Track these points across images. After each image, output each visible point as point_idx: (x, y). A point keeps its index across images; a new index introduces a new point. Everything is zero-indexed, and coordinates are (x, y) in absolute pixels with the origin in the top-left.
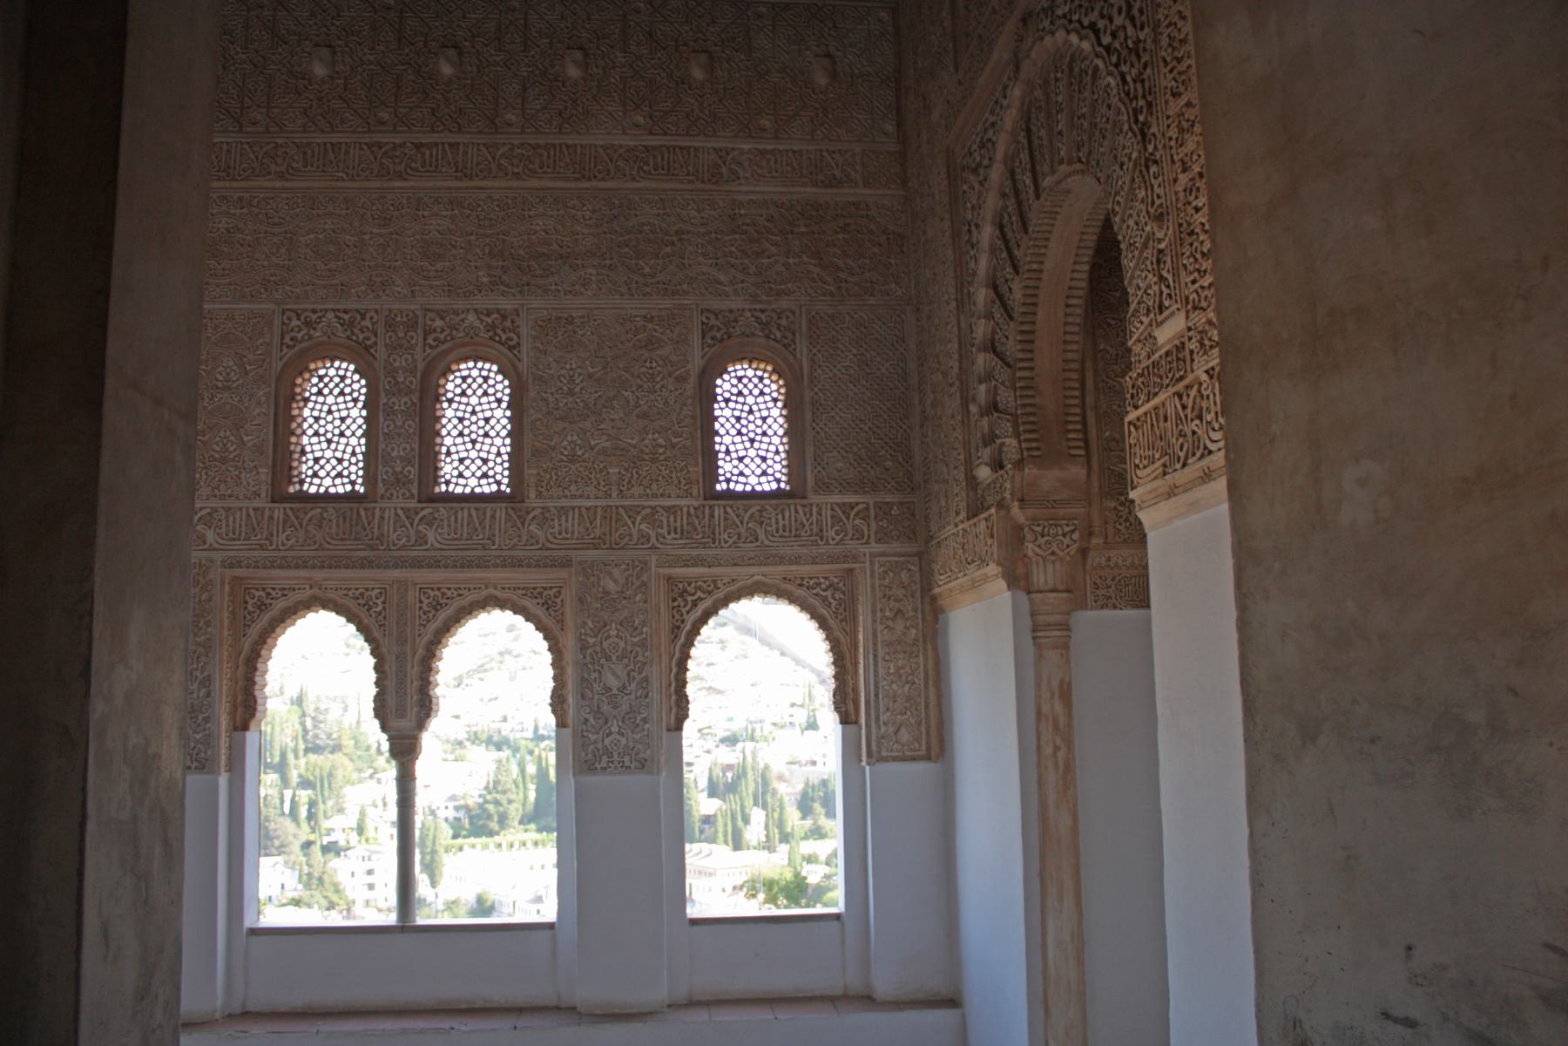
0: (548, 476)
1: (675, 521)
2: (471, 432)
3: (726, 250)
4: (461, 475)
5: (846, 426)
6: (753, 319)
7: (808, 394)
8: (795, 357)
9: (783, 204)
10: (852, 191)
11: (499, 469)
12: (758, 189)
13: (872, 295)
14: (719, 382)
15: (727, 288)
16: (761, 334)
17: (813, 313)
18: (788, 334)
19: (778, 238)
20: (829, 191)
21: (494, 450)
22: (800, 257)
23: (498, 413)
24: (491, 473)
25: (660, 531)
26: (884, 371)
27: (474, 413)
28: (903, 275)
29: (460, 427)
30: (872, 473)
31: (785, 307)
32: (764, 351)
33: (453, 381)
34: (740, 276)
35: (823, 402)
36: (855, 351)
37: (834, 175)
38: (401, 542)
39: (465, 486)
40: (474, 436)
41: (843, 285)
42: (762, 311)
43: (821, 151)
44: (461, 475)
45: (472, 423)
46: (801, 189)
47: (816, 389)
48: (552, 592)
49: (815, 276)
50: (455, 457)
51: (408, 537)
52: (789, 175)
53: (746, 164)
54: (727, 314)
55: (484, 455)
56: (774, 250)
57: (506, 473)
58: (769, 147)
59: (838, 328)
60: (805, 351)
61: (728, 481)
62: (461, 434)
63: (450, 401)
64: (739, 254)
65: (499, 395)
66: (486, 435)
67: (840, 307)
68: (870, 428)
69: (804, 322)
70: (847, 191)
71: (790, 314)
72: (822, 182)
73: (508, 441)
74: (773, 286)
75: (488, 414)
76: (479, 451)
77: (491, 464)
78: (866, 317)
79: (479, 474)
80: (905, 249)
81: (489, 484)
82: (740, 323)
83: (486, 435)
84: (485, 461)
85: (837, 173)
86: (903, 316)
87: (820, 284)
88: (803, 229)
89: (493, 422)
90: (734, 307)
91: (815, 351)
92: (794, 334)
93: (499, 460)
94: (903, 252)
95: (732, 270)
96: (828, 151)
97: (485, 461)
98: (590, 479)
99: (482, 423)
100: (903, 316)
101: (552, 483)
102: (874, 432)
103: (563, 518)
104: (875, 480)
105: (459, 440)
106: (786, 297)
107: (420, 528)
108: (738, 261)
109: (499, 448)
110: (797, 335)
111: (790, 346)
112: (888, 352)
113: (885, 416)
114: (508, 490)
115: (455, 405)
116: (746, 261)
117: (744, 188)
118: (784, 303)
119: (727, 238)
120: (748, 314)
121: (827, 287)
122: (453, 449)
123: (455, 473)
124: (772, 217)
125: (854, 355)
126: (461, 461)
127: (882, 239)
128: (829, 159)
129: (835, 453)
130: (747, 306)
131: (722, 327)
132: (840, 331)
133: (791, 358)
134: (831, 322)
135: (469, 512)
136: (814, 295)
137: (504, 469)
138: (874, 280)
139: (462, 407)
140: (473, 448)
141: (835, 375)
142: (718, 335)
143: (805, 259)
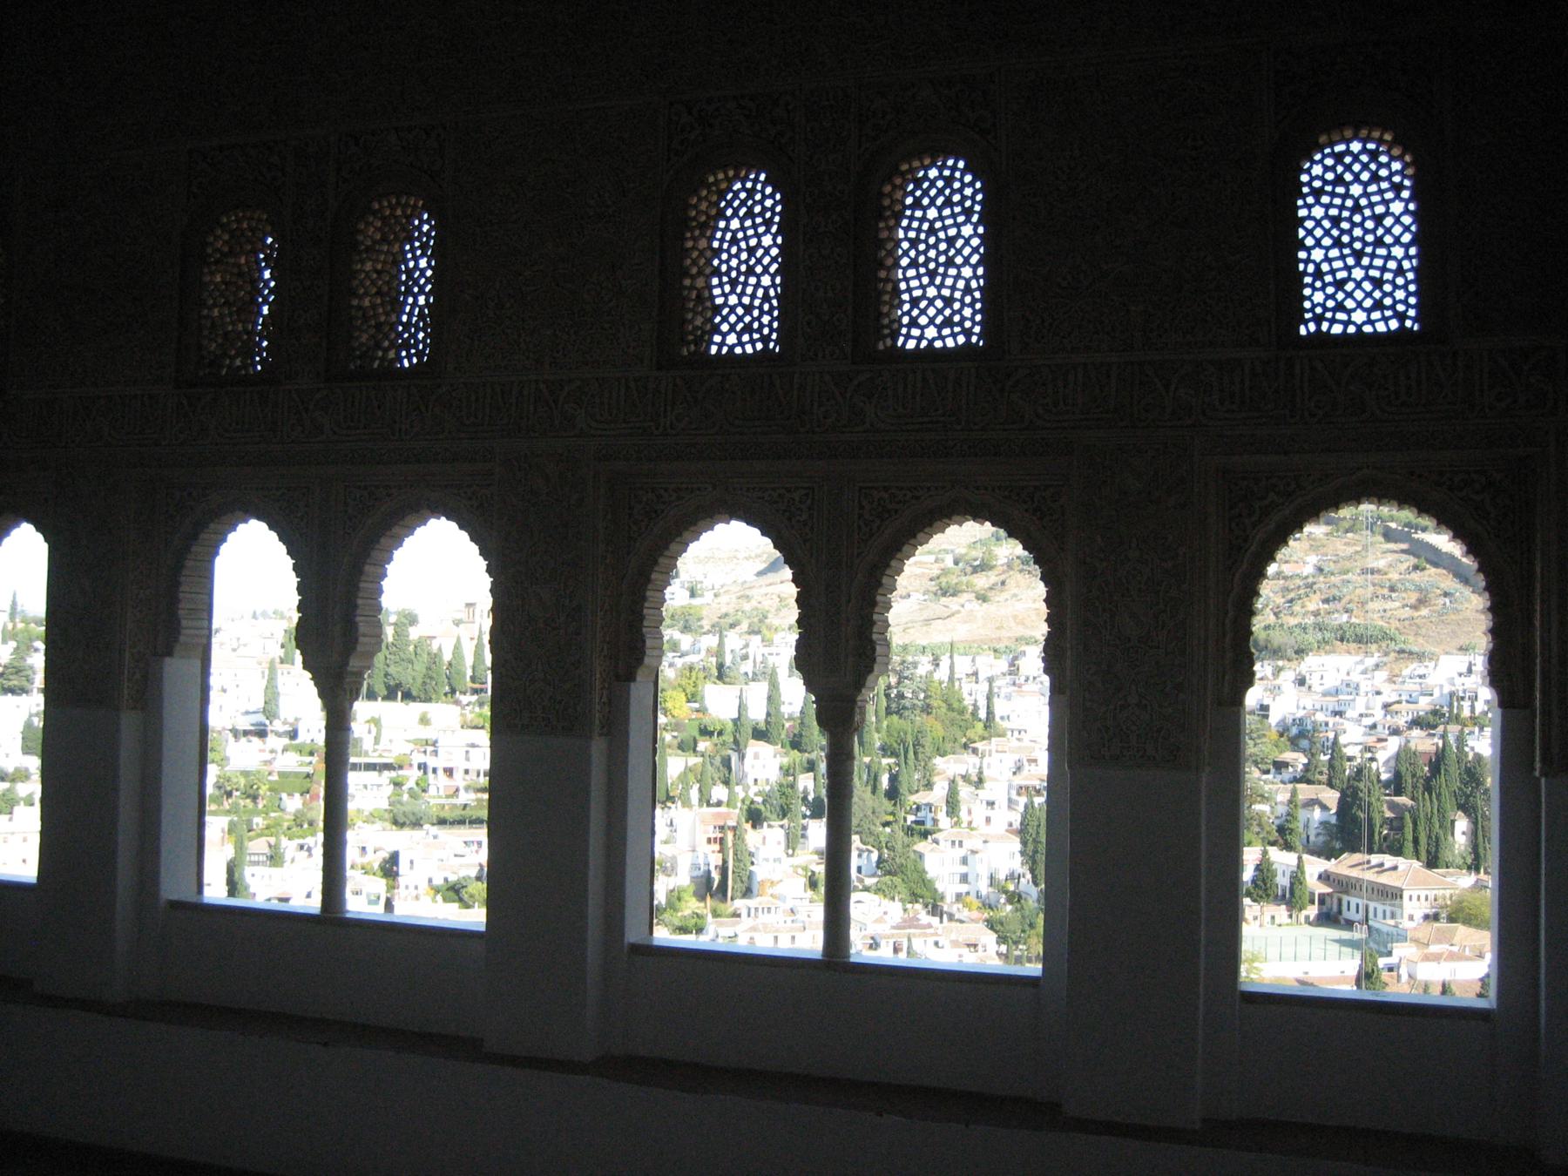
2: (1353, 240)
4: (1340, 307)
21: (1392, 265)
23: (1397, 207)
24: (1388, 301)
27: (1357, 208)
33: (1321, 161)
39: (1346, 324)
40: (1358, 245)
44: (1340, 307)
45: (1354, 225)
50: (1328, 279)
55: (1374, 273)
57: (1412, 300)
62: (1337, 243)
63: (1317, 193)
66: (1379, 242)
73: (1413, 251)
75: (1380, 209)
77: (1388, 288)
79: (1368, 303)
81: (1385, 319)
83: (1379, 242)
84: (1379, 284)
89: (1388, 221)
93: (1400, 281)
99: (1370, 225)
105: (1334, 253)
115: (1325, 199)
126: (1339, 285)
137: (1409, 294)
139: (1337, 201)
140: (1358, 264)
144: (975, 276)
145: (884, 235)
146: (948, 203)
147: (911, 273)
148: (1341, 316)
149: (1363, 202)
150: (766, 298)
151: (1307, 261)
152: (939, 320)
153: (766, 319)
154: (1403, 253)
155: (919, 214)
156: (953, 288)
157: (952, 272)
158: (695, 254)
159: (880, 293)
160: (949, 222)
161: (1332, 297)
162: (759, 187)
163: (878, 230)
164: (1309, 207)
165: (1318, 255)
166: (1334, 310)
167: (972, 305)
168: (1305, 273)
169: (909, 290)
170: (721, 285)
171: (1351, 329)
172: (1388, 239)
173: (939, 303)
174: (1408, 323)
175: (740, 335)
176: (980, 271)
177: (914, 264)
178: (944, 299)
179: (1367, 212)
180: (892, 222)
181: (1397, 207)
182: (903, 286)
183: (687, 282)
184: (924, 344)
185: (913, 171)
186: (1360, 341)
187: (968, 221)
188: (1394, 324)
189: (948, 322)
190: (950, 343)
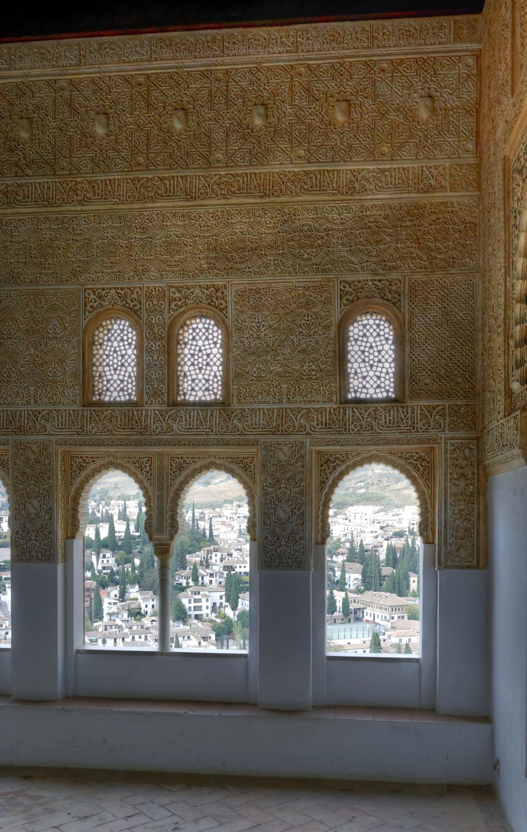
0: (294, 389)
4: (364, 387)
10: (442, 194)
13: (453, 267)
14: (351, 328)
15: (357, 266)
17: (413, 281)
18: (396, 295)
19: (392, 231)
21: (384, 370)
22: (405, 243)
25: (380, 422)
26: (459, 318)
27: (371, 347)
29: (363, 357)
31: (394, 277)
34: (365, 258)
35: (418, 340)
36: (440, 306)
39: (367, 394)
40: (371, 362)
41: (434, 260)
42: (380, 281)
44: (364, 387)
45: (370, 354)
49: (415, 255)
51: (294, 426)
54: (357, 284)
55: (378, 374)
56: (388, 239)
59: (429, 290)
60: (407, 307)
62: (364, 361)
63: (356, 340)
65: (387, 336)
67: (431, 276)
70: (438, 194)
71: (397, 282)
76: (375, 372)
78: (448, 282)
79: (375, 386)
80: (477, 234)
81: (382, 392)
82: (365, 289)
84: (379, 378)
86: (474, 280)
87: (418, 261)
88: (408, 224)
90: (361, 278)
91: (413, 306)
92: (400, 295)
93: (387, 377)
97: (379, 378)
98: (319, 390)
99: (376, 354)
103: (387, 415)
105: (362, 365)
106: (395, 271)
107: (368, 420)
109: (387, 369)
110: (402, 296)
112: (462, 305)
114: (393, 396)
115: (359, 343)
116: (370, 247)
118: (394, 275)
120: (370, 283)
123: (360, 386)
127: (461, 227)
130: (370, 278)
131: (353, 292)
132: (431, 292)
133: (397, 311)
135: (398, 409)
138: (455, 256)
139: (364, 344)
141: (426, 322)
143: (409, 244)
145: (180, 351)
146: (207, 339)
147: (192, 368)
148: (364, 390)
149: (374, 345)
150: (130, 377)
151: (351, 368)
152: (203, 388)
153: (130, 386)
155: (194, 343)
157: (209, 368)
158: (98, 357)
159: (178, 377)
160: (207, 347)
161: (361, 383)
162: (126, 328)
164: (353, 346)
165: (356, 365)
166: (362, 388)
167: (217, 382)
168: (351, 373)
169: (191, 375)
170: (110, 370)
171: (368, 396)
172: (383, 360)
173: (204, 381)
174: (390, 394)
175: (119, 392)
177: (193, 364)
179: (375, 349)
180: (183, 346)
182: (188, 374)
183: (95, 369)
185: (191, 324)
186: (371, 401)
187: (215, 347)
188: (385, 394)
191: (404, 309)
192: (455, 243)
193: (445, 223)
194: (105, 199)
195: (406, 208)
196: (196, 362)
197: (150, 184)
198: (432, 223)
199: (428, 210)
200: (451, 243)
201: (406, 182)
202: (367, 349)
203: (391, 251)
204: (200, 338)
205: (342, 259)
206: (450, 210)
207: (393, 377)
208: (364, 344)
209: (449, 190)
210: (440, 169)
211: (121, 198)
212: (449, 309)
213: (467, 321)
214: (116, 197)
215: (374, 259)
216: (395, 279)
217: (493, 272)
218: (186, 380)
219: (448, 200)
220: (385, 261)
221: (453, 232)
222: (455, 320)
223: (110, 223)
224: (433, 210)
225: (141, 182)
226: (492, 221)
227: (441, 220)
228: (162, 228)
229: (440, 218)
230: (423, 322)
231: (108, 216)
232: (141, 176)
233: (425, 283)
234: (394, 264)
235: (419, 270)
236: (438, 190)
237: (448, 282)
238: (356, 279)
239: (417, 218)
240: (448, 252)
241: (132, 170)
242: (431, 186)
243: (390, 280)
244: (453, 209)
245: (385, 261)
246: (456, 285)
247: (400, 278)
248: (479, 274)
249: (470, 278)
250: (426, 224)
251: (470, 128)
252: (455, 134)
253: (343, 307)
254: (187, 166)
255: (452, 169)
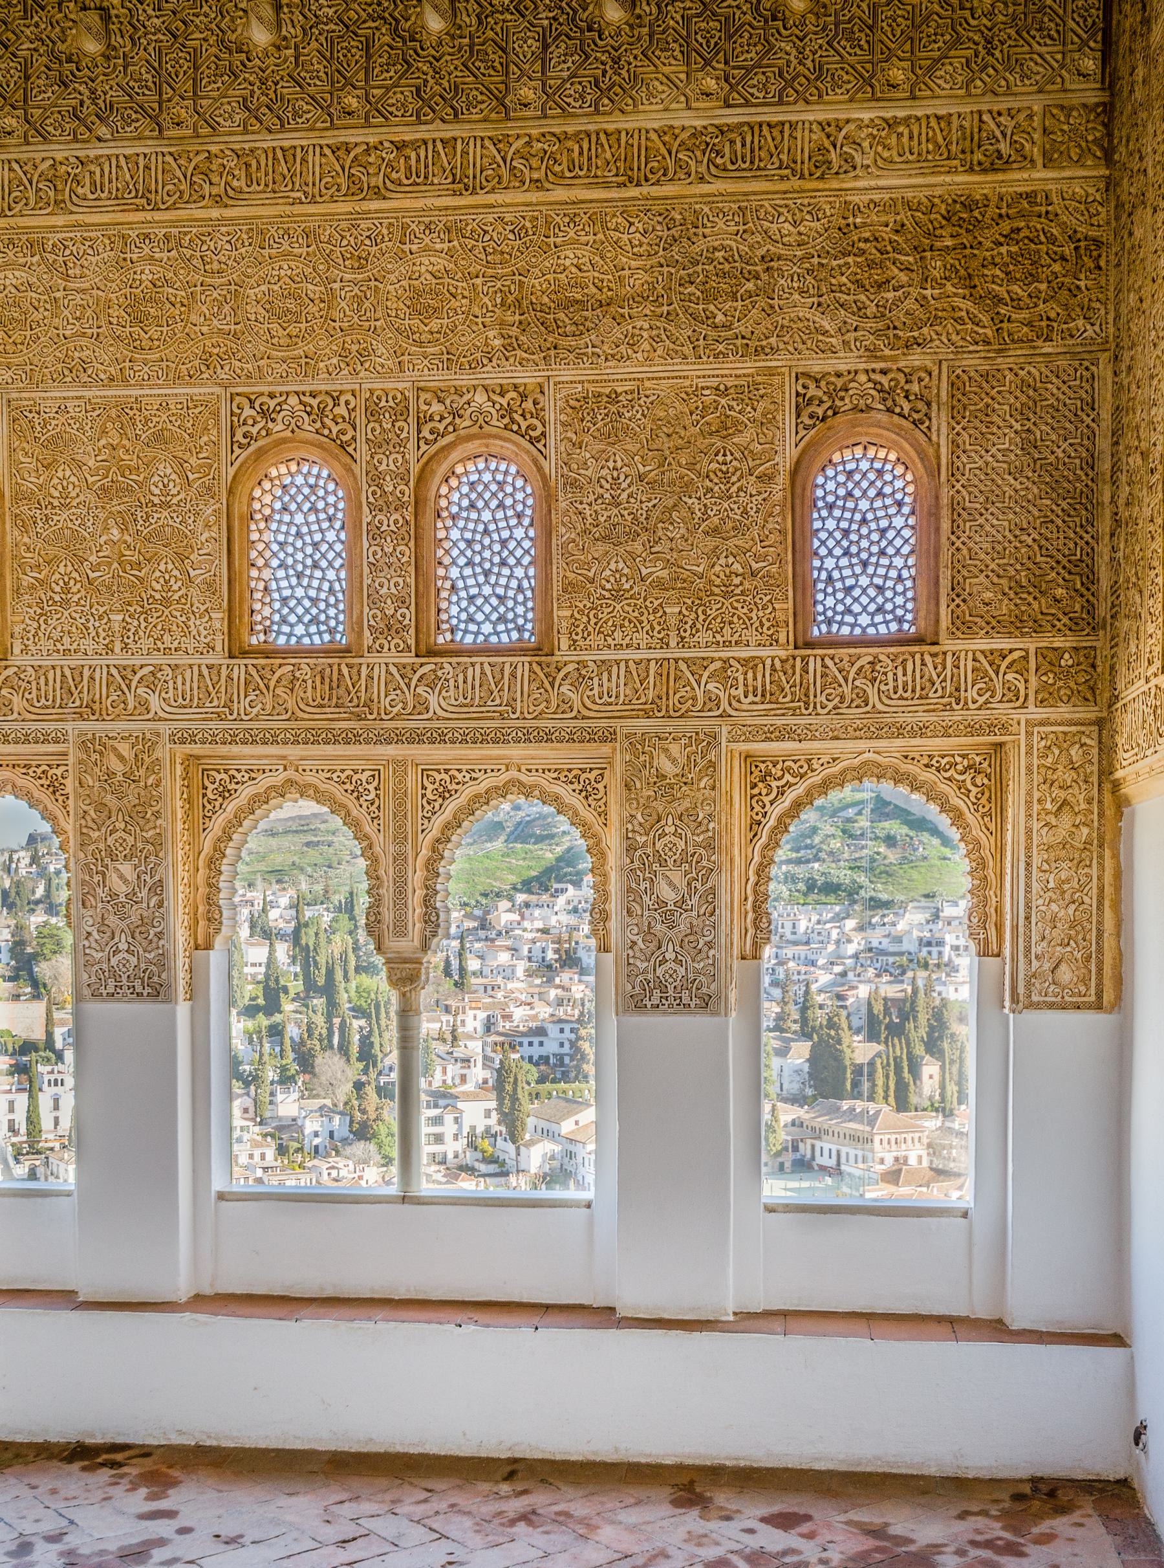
0: (585, 619)
1: (755, 679)
3: (834, 281)
5: (1001, 539)
6: (871, 385)
7: (945, 494)
8: (930, 439)
9: (919, 203)
10: (1026, 176)
11: (520, 610)
12: (882, 183)
13: (1048, 339)
14: (820, 480)
15: (833, 340)
16: (881, 407)
17: (959, 371)
18: (920, 405)
19: (911, 259)
20: (990, 177)
21: (514, 584)
23: (519, 533)
25: (733, 692)
26: (1061, 455)
28: (1098, 305)
30: (1035, 605)
31: (917, 363)
32: (885, 433)
34: (853, 321)
35: (967, 504)
36: (1017, 426)
37: (998, 151)
38: (395, 710)
41: (1005, 325)
42: (884, 372)
43: (980, 113)
46: (948, 179)
47: (958, 486)
48: (592, 776)
52: (930, 157)
53: (866, 144)
54: (833, 379)
56: (903, 277)
58: (901, 114)
59: (993, 392)
60: (944, 430)
61: (829, 622)
62: (470, 563)
64: (852, 287)
67: (999, 360)
68: (1034, 540)
69: (944, 385)
70: (1017, 175)
71: (923, 375)
72: (980, 163)
74: (901, 334)
80: (1102, 263)
82: (851, 392)
85: (1004, 147)
86: (1093, 368)
88: (949, 242)
90: (843, 368)
91: (958, 428)
92: (929, 404)
94: (1100, 268)
95: (843, 312)
96: (990, 112)
97: (502, 599)
98: (641, 622)
99: (497, 547)
100: (1093, 368)
101: (590, 629)
102: (1040, 547)
103: (605, 676)
104: (1040, 616)
105: (468, 571)
106: (919, 350)
108: (851, 298)
110: (934, 406)
111: (922, 423)
112: (1068, 425)
113: (1059, 522)
115: (461, 524)
116: (863, 297)
117: (861, 184)
118: (916, 359)
119: (835, 263)
120: (863, 378)
121: (981, 331)
122: (836, 575)
123: (464, 616)
124: (903, 225)
125: (1016, 432)
126: (471, 599)
128: (993, 126)
129: (982, 577)
130: (862, 366)
131: (825, 398)
133: (922, 438)
134: (984, 384)
136: (961, 343)
138: (1053, 315)
142: (820, 413)
143: (949, 288)
144: (339, 580)
145: (255, 536)
146: (314, 509)
147: (281, 573)
150: (331, 591)
154: (524, 573)
156: (319, 589)
163: (249, 531)
166: (466, 622)
169: (279, 589)
172: (512, 561)
176: (343, 575)
178: (310, 599)
181: (519, 533)
184: (293, 640)
189: (315, 620)
190: (317, 640)
191: (938, 435)
192: (1054, 284)
193: (1032, 241)
194: (275, 192)
195: (943, 206)
196: (290, 561)
197: (371, 160)
198: (1002, 240)
199: (992, 211)
200: (1043, 286)
201: (775, 159)
202: (478, 537)
203: (909, 304)
204: (299, 508)
205: (801, 325)
206: (1043, 209)
207: (533, 599)
208: (471, 526)
209: (1039, 162)
210: (1022, 117)
211: (309, 189)
212: (1038, 434)
213: (1077, 461)
214: (297, 186)
215: (871, 324)
216: (919, 369)
217: (1140, 349)
218: (267, 600)
219: (1037, 187)
220: (895, 328)
221: (1049, 261)
222: (1052, 459)
223: (286, 246)
224: (1003, 211)
225: (352, 155)
226: (1138, 233)
227: (1022, 235)
228: (400, 257)
229: (1019, 230)
230: (981, 463)
231: (281, 232)
232: (353, 140)
233: (985, 376)
234: (916, 334)
235: (971, 348)
236: (1015, 166)
237: (1037, 374)
238: (830, 370)
239: (968, 231)
240: (1036, 306)
241: (333, 127)
242: (1000, 157)
243: (907, 370)
244: (1050, 208)
245: (895, 328)
246: (1055, 380)
247: (929, 364)
248: (1107, 354)
249: (1086, 363)
250: (989, 244)
251: (1090, 20)
252: (1056, 36)
253: (424, 447)
254: (456, 115)
255: (1048, 115)
